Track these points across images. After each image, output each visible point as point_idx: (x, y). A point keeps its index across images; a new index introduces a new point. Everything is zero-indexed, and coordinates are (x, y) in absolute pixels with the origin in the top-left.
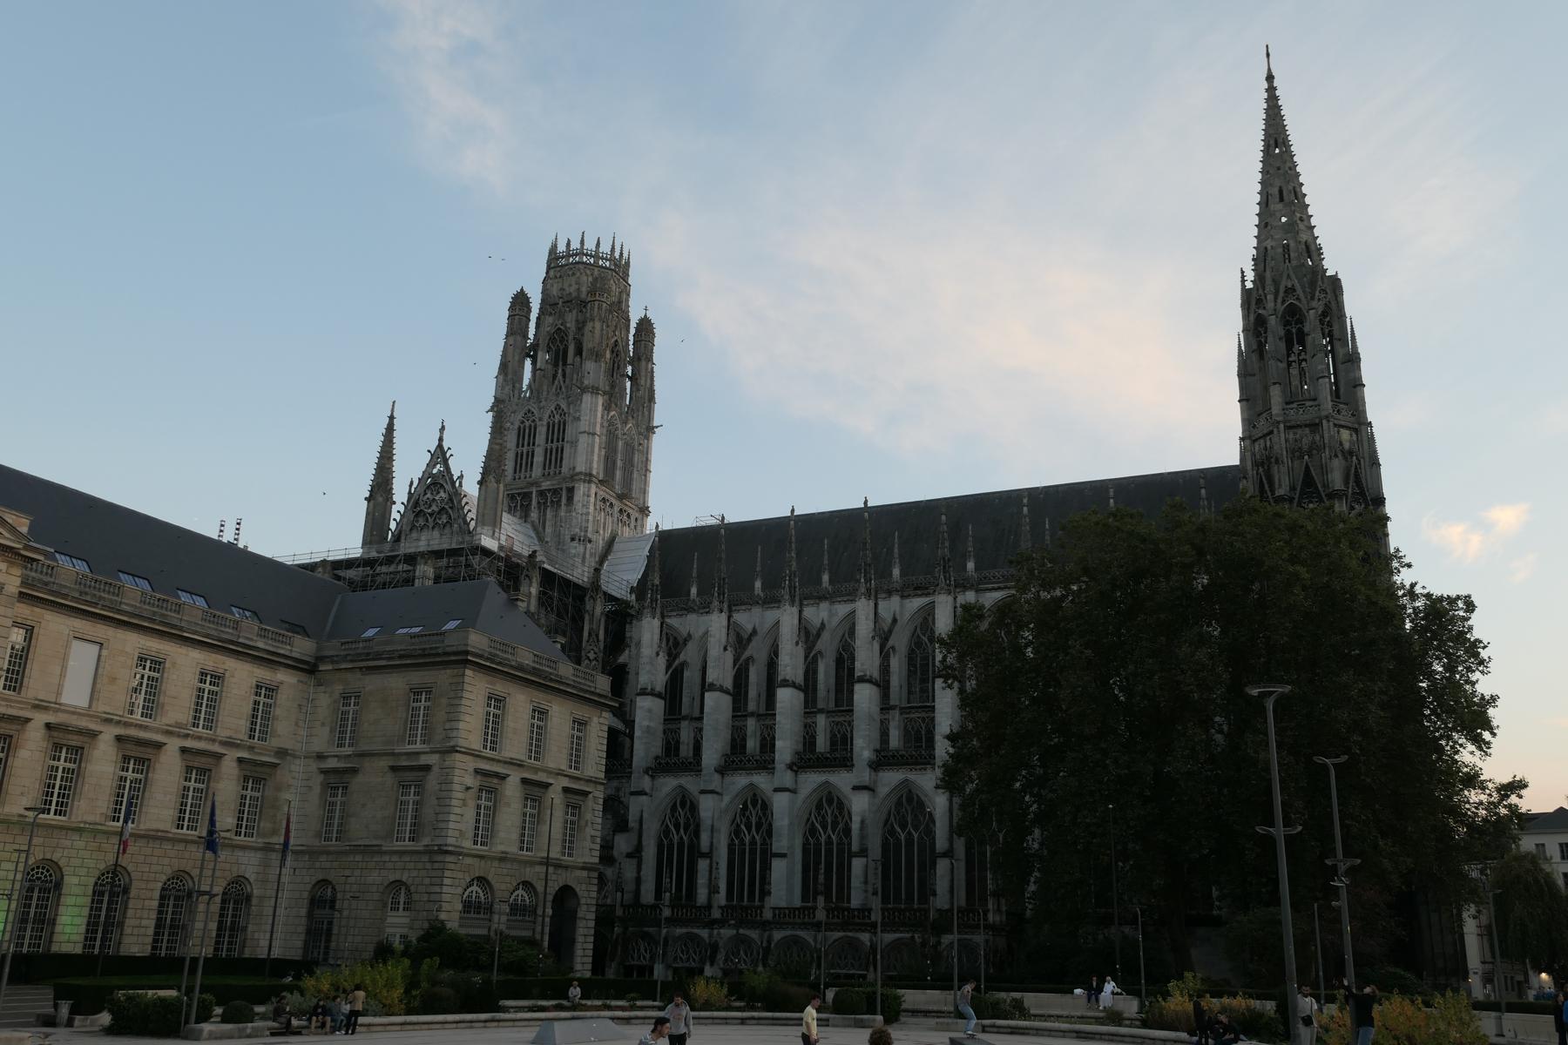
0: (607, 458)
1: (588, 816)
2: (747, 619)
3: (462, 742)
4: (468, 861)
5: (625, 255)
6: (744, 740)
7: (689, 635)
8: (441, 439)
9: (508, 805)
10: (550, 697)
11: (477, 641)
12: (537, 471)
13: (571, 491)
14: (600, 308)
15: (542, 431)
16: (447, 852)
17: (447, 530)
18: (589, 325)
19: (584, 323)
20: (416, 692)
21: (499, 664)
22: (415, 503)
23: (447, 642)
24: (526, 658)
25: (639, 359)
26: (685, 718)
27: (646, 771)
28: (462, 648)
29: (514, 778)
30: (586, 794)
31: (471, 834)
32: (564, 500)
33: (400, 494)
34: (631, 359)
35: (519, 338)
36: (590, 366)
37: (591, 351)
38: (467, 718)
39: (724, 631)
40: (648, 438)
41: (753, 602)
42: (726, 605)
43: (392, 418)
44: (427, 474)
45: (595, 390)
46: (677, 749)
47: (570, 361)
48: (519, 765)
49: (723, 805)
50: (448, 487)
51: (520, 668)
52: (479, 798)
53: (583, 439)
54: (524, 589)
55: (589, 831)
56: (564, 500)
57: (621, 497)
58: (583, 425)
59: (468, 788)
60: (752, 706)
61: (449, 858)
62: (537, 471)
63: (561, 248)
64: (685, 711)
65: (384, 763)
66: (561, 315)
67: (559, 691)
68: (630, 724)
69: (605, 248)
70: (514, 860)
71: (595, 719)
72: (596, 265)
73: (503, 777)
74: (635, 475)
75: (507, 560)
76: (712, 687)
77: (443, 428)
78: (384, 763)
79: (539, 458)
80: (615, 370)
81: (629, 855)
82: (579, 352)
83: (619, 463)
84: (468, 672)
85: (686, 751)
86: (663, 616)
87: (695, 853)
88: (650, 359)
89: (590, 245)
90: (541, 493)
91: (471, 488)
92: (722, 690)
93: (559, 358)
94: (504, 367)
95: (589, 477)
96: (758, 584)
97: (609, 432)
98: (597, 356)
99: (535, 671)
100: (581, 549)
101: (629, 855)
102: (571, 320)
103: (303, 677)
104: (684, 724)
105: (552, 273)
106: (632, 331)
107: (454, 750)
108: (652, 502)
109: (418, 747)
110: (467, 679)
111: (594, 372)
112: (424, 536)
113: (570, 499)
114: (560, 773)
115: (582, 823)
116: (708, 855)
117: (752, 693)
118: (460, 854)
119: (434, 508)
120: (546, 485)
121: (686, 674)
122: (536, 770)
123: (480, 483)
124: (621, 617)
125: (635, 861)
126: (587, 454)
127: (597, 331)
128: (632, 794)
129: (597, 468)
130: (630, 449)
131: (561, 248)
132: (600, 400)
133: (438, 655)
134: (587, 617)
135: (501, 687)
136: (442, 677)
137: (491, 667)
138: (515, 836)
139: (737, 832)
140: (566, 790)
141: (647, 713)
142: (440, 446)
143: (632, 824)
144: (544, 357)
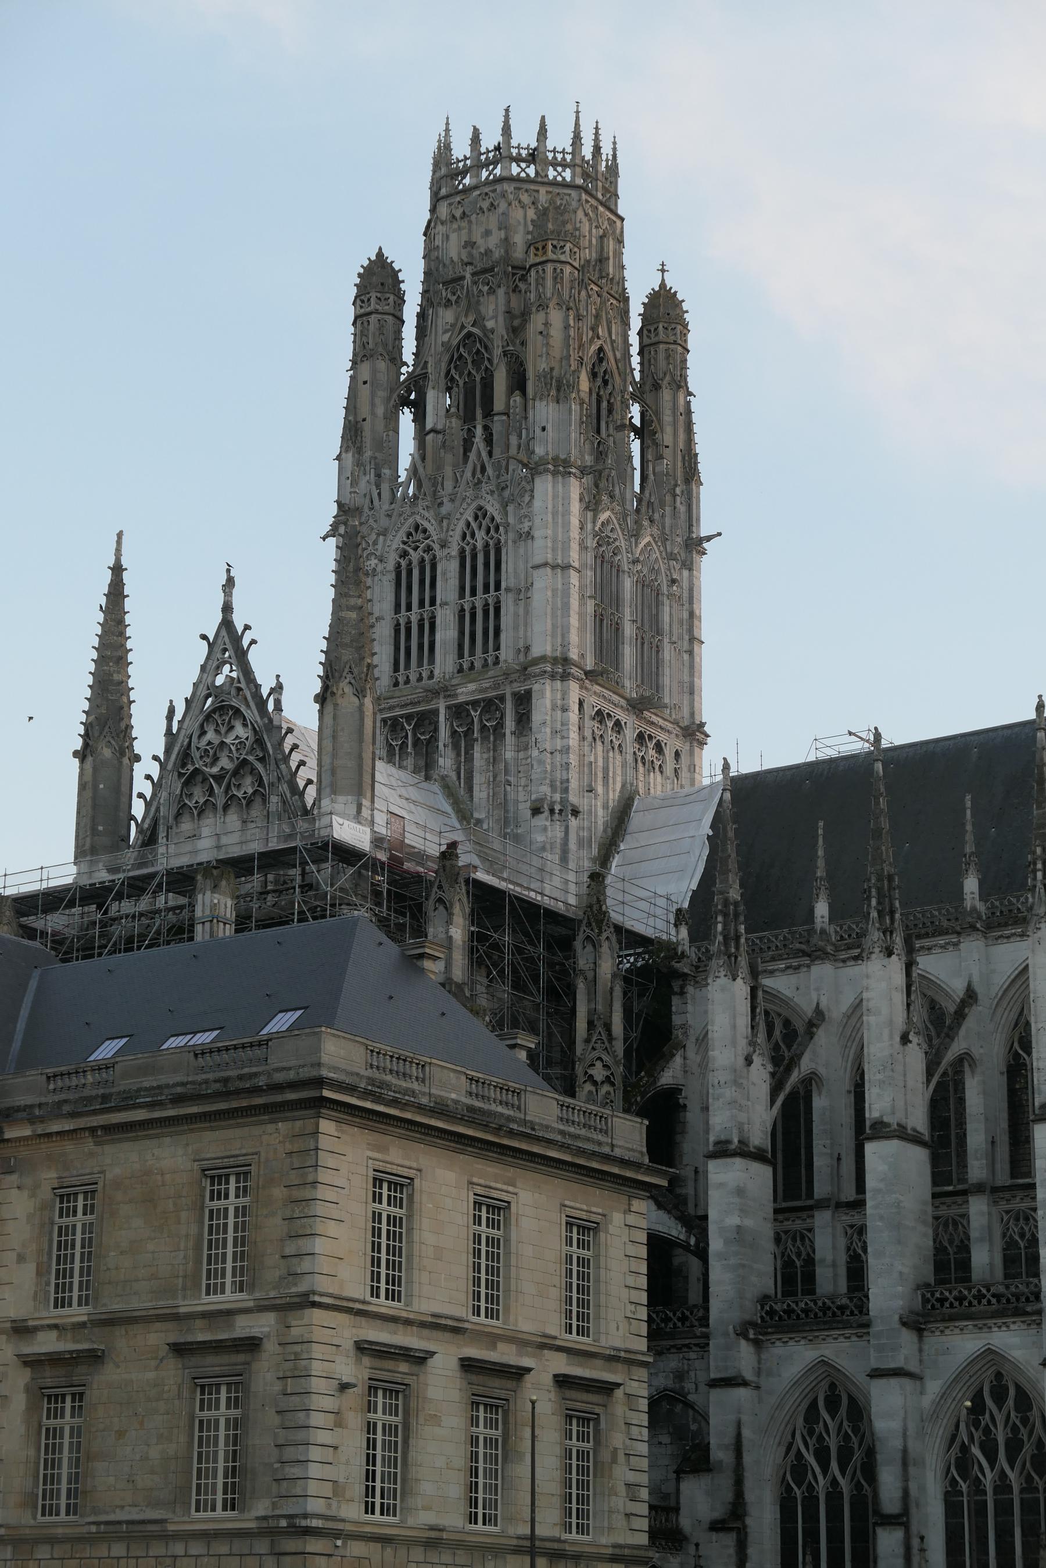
0: (599, 619)
1: (618, 1439)
2: (949, 967)
3: (323, 1284)
4: (357, 1549)
5: (606, 150)
6: (964, 1248)
7: (819, 1012)
8: (227, 608)
9: (435, 1420)
10: (511, 1172)
11: (339, 1054)
12: (445, 662)
13: (524, 700)
14: (557, 278)
15: (448, 571)
16: (308, 1531)
17: (256, 811)
18: (537, 320)
19: (525, 315)
20: (215, 1176)
21: (394, 1103)
22: (182, 758)
23: (274, 1062)
24: (450, 1086)
25: (657, 387)
26: (822, 1204)
27: (742, 1334)
28: (306, 1073)
29: (445, 1359)
30: (607, 1388)
31: (358, 1489)
32: (510, 724)
33: (149, 738)
34: (635, 394)
35: (382, 365)
36: (544, 412)
37: (546, 377)
38: (332, 1229)
39: (900, 998)
40: (689, 566)
41: (958, 926)
42: (898, 940)
43: (117, 570)
44: (204, 688)
45: (561, 467)
46: (810, 1278)
47: (499, 405)
49: (927, 1401)
50: (251, 714)
51: (440, 1110)
52: (371, 1407)
53: (543, 580)
54: (434, 930)
55: (622, 1474)
56: (510, 724)
57: (638, 706)
58: (541, 549)
59: (344, 1387)
60: (977, 1170)
61: (314, 1545)
62: (445, 662)
63: (461, 149)
64: (821, 1189)
65: (158, 1337)
66: (472, 305)
67: (532, 1156)
68: (698, 1224)
69: (559, 140)
70: (457, 1545)
71: (617, 1218)
72: (540, 180)
73: (420, 1359)
74: (667, 653)
76: (881, 1131)
77: (230, 582)
78: (158, 1337)
79: (446, 633)
80: (602, 414)
81: (716, 1526)
82: (519, 383)
83: (629, 630)
84: (326, 1126)
85: (830, 1280)
86: (754, 973)
87: (868, 1516)
88: (680, 383)
89: (524, 137)
90: (458, 712)
91: (300, 711)
92: (903, 1134)
93: (475, 403)
94: (353, 432)
95: (561, 667)
96: (971, 885)
97: (601, 559)
98: (560, 388)
99: (473, 1116)
100: (556, 831)
101: (716, 1526)
102: (494, 311)
104: (822, 1219)
105: (443, 210)
106: (636, 323)
107: (306, 1302)
108: (712, 710)
109: (229, 1298)
110: (324, 1142)
111: (555, 425)
112: (208, 826)
113: (524, 719)
114: (546, 1344)
115: (605, 1456)
116: (900, 1520)
117: (976, 1138)
118: (337, 1534)
119: (225, 762)
120: (467, 691)
121: (819, 1103)
122: (492, 1339)
123: (321, 699)
124: (658, 981)
125: (729, 1540)
126: (552, 614)
127: (556, 333)
128: (714, 1384)
129: (580, 645)
130: (651, 595)
131: (461, 149)
132: (575, 488)
133: (257, 1090)
134: (581, 986)
135: (400, 1155)
136: (268, 1141)
137: (376, 1113)
138: (455, 1489)
139: (963, 1463)
140: (562, 1381)
141: (735, 1196)
142: (227, 623)
143: (720, 1454)
144: (439, 402)
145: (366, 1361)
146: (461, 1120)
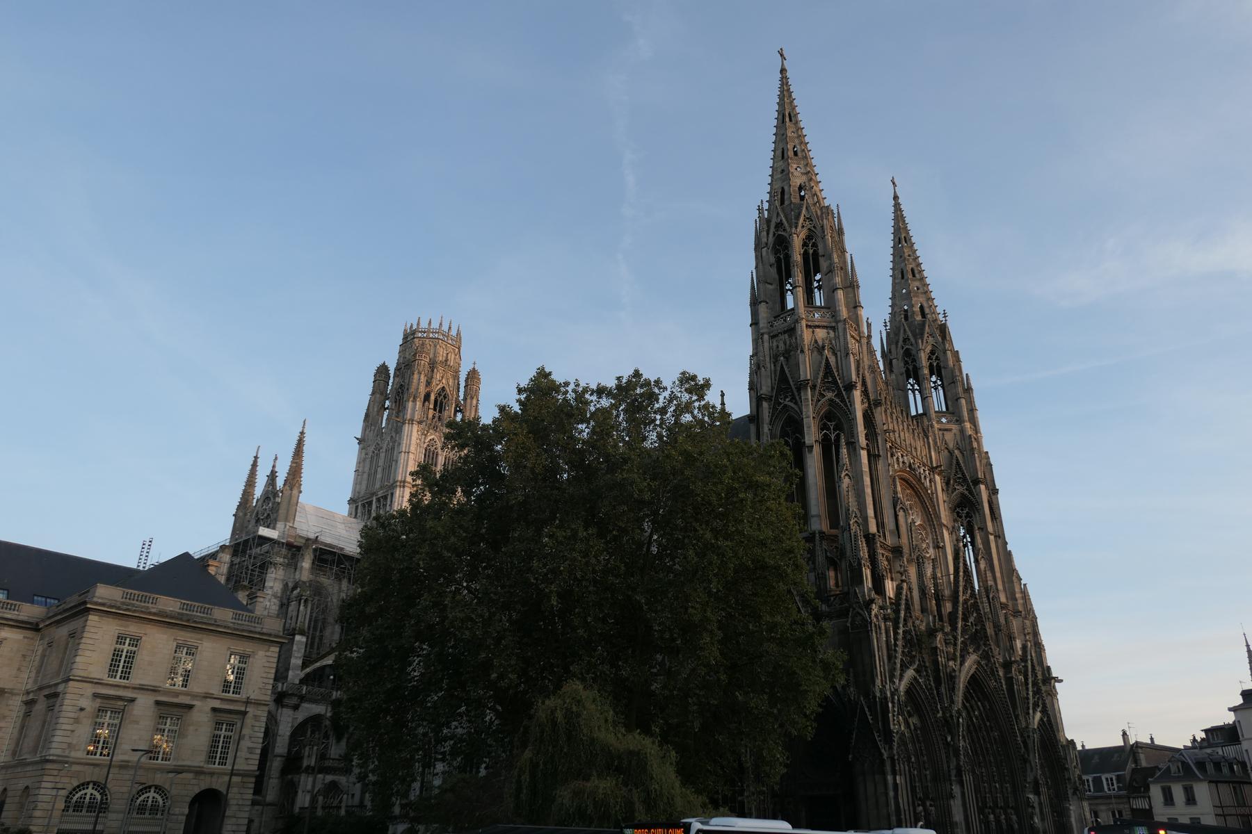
4: (75, 768)
10: (200, 636)
16: (48, 761)
38: (88, 653)
48: (155, 690)
59: (82, 709)
61: (49, 766)
73: (132, 700)
75: (290, 546)
99: (180, 616)
103: (29, 634)
114: (207, 696)
145: (99, 700)
146: (172, 618)
